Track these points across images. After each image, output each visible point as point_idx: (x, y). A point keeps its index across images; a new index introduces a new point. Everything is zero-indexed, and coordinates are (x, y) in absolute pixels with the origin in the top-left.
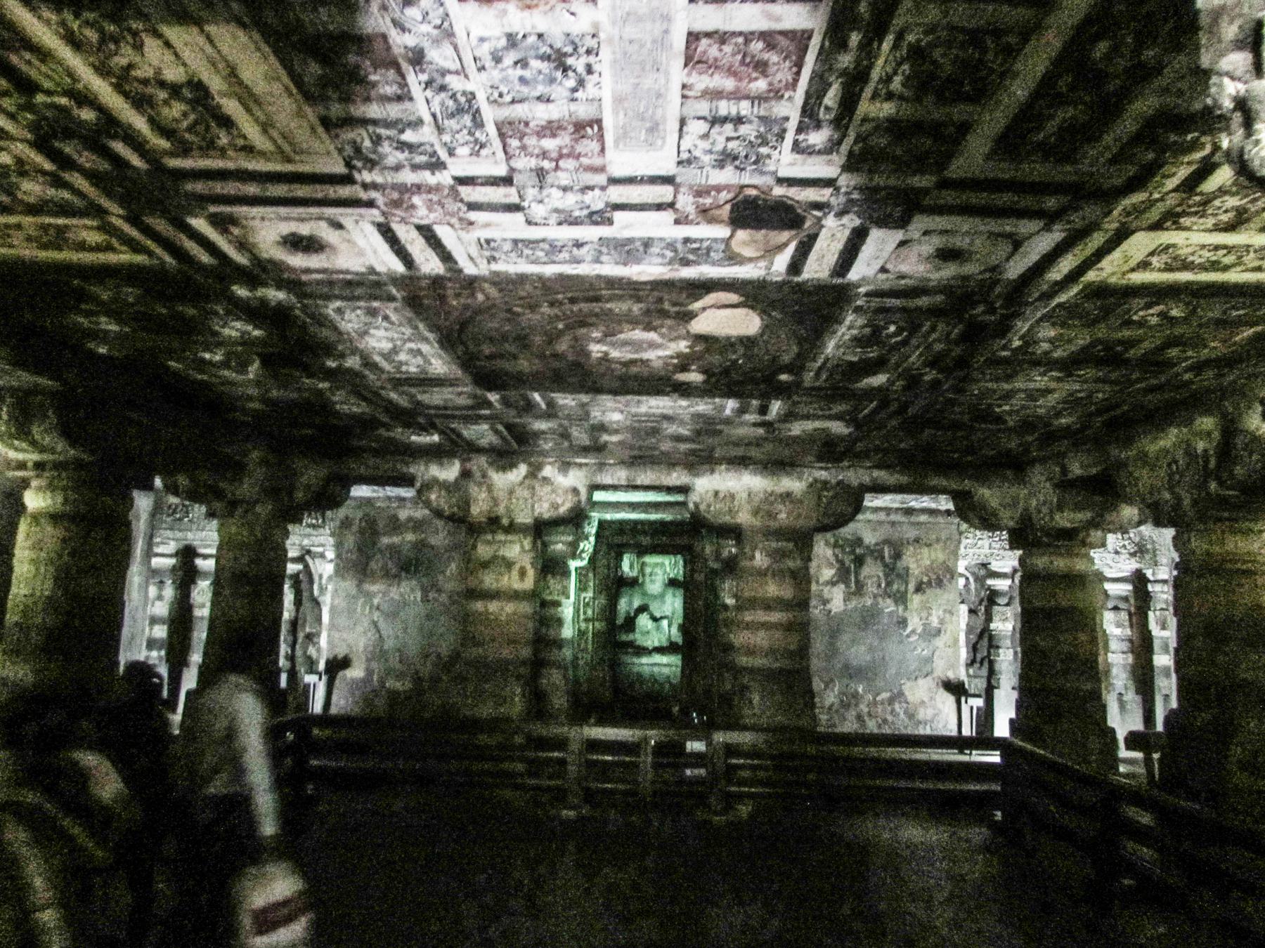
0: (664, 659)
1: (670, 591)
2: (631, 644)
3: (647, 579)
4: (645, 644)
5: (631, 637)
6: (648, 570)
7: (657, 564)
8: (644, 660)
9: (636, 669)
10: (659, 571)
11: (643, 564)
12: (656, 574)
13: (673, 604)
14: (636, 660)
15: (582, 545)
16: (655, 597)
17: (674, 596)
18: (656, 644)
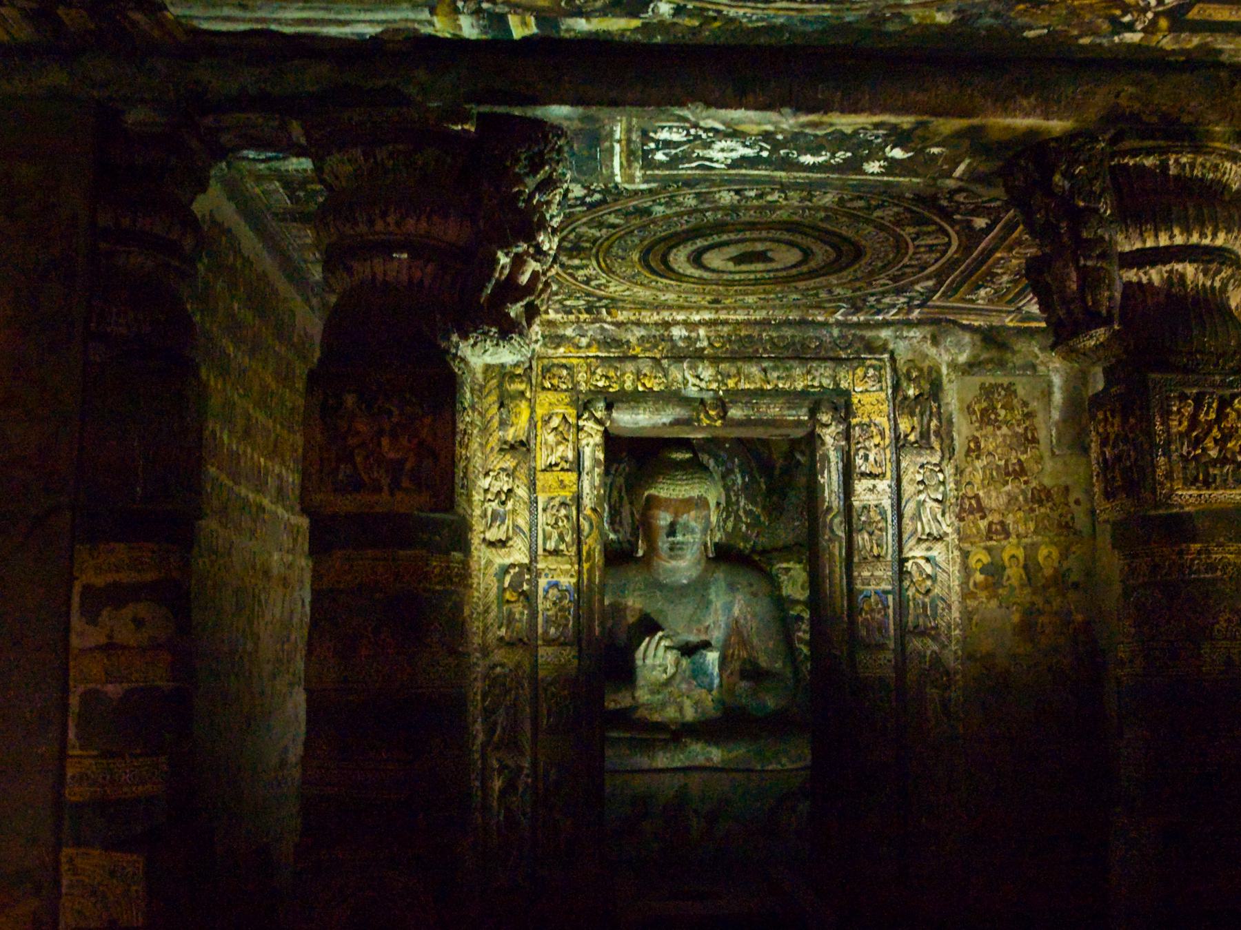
0: (716, 755)
1: (720, 575)
2: (624, 718)
3: (663, 543)
4: (656, 717)
5: (624, 700)
6: (664, 519)
7: (689, 504)
8: (662, 760)
9: (639, 783)
10: (690, 518)
11: (652, 503)
12: (687, 529)
13: (728, 607)
14: (643, 761)
15: (504, 260)
16: (679, 592)
17: (732, 587)
18: (690, 714)
